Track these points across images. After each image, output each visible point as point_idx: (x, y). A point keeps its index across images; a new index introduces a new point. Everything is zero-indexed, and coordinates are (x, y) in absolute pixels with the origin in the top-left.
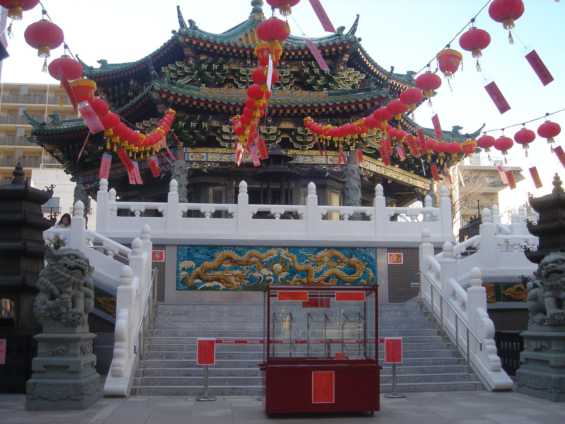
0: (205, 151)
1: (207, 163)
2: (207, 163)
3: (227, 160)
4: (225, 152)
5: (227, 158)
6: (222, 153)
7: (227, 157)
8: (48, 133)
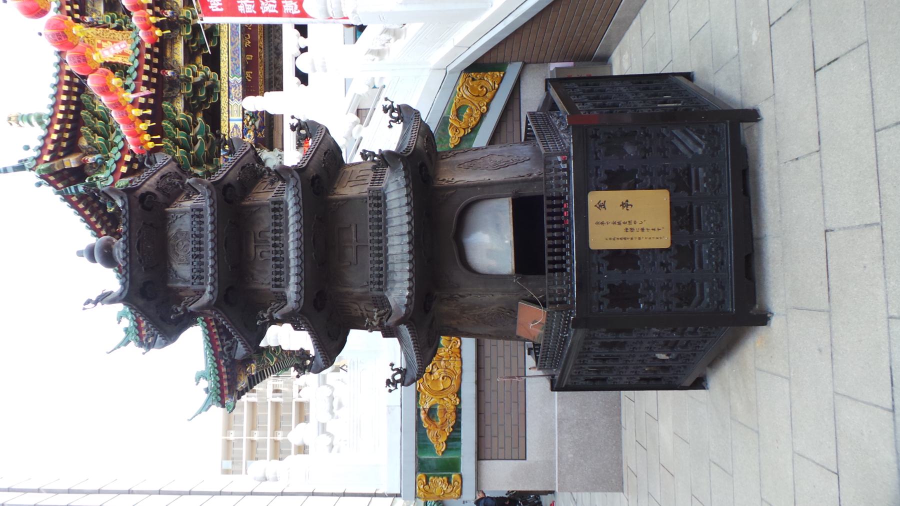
0: (227, 123)
1: (245, 122)
2: (245, 122)
3: (239, 89)
4: (227, 93)
5: (237, 90)
6: (229, 98)
7: (235, 89)
8: (218, 382)
